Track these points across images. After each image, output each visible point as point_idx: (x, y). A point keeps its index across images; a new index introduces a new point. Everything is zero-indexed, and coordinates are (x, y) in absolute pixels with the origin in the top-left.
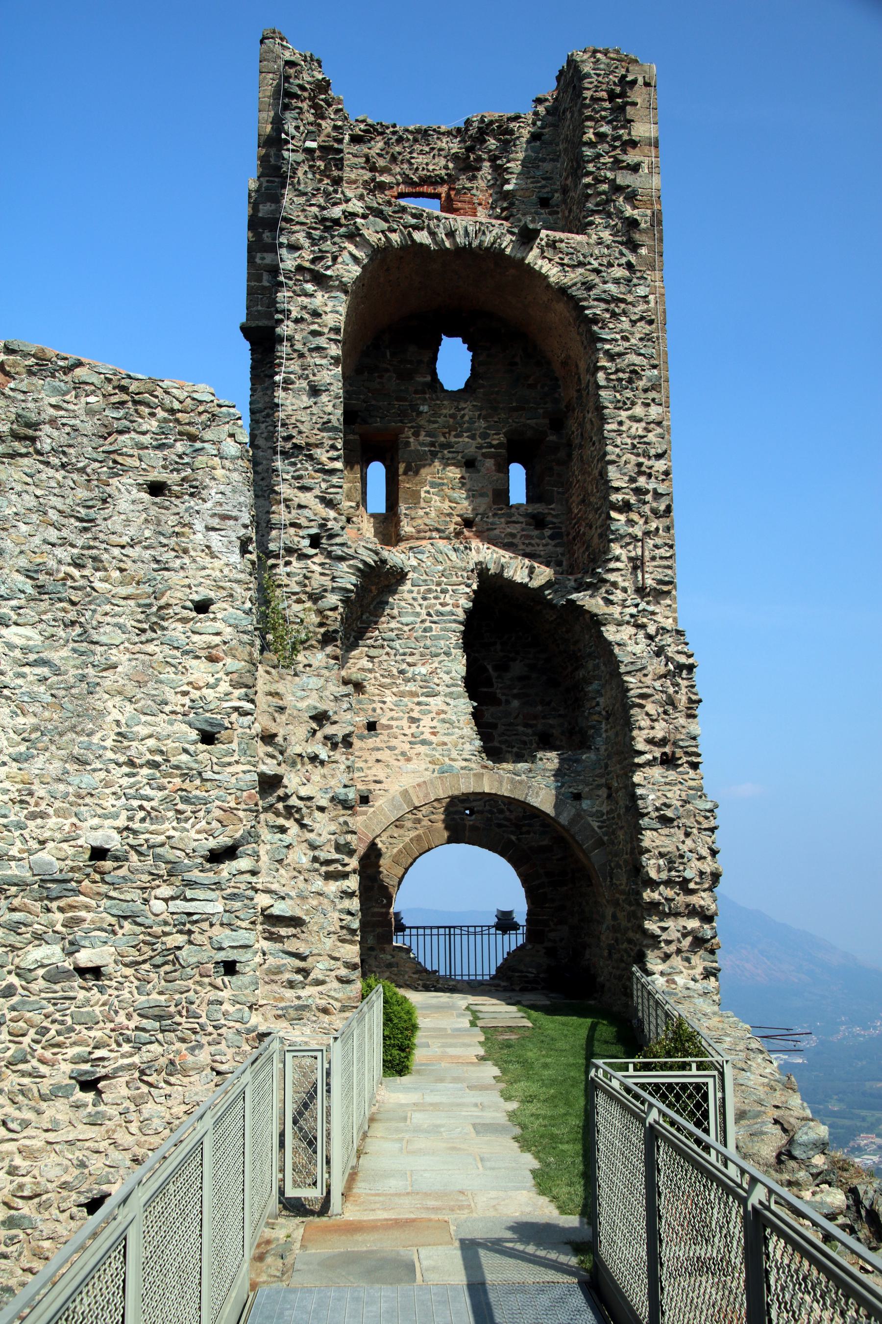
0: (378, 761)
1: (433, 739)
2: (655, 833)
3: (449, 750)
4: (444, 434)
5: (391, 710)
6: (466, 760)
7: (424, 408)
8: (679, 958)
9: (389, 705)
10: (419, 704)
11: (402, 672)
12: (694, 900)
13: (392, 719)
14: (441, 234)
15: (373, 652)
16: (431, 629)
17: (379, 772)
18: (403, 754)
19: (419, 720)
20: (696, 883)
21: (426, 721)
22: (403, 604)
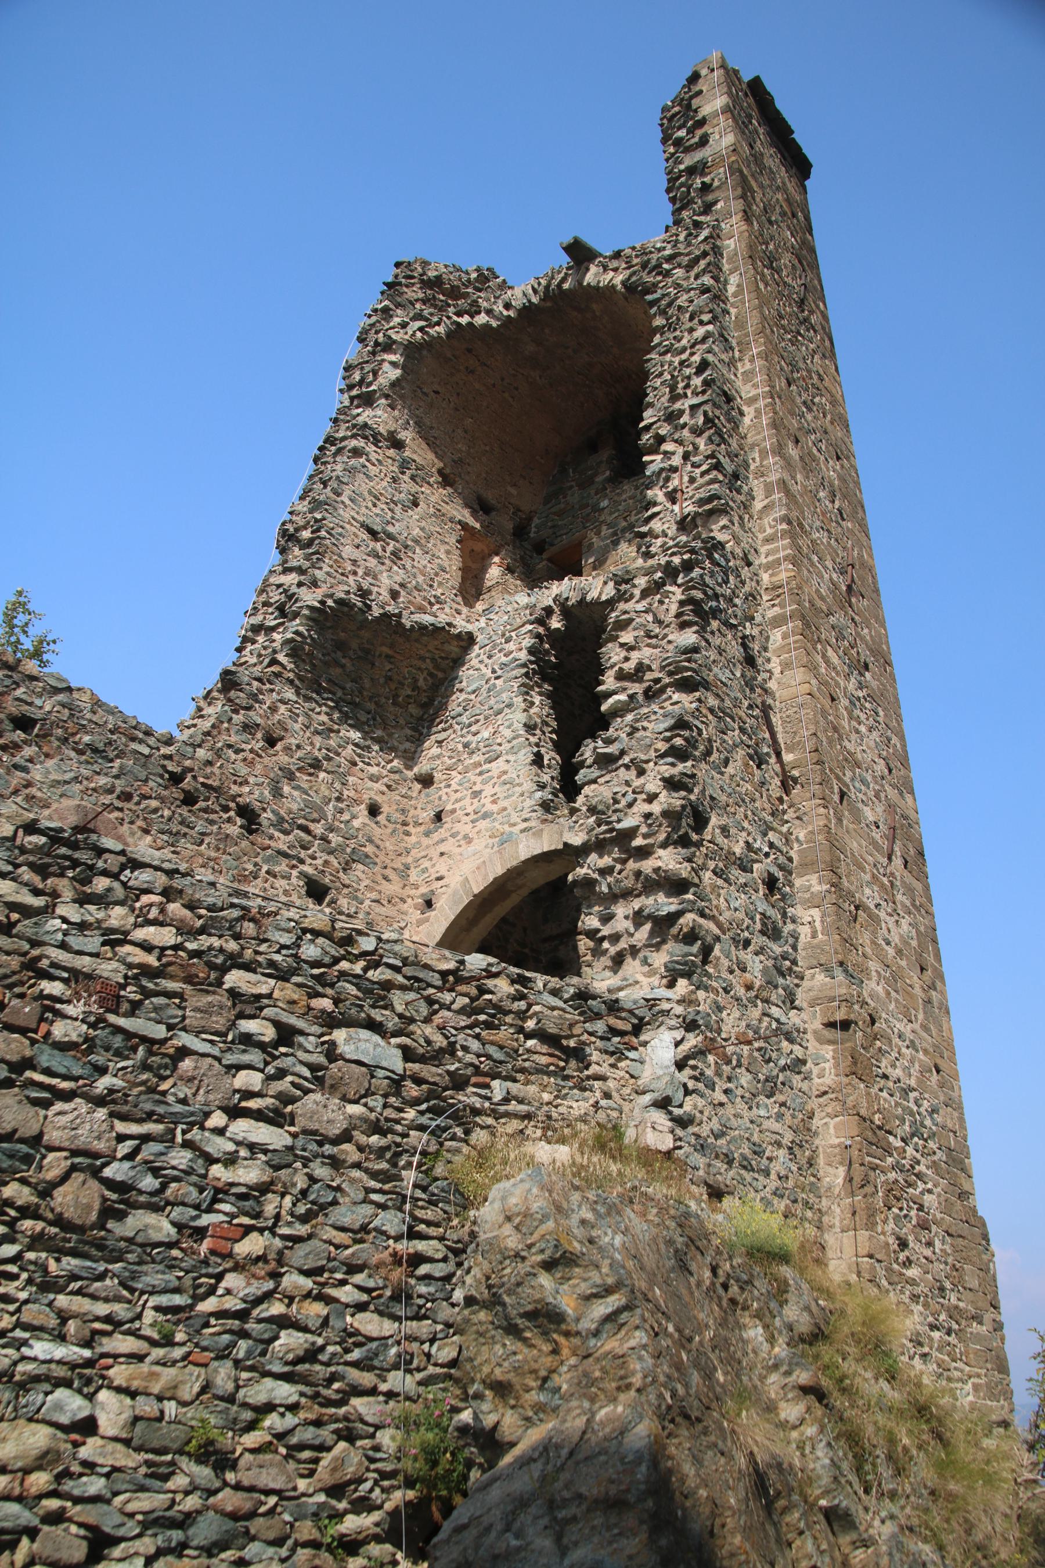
0: (442, 854)
1: (495, 808)
2: (593, 786)
3: (509, 815)
4: (625, 519)
5: (456, 791)
6: (525, 820)
7: (605, 503)
8: (637, 962)
9: (454, 786)
10: (481, 774)
11: (466, 746)
12: (647, 866)
13: (457, 801)
14: (499, 308)
15: (441, 736)
16: (494, 685)
17: (441, 867)
18: (466, 837)
19: (480, 792)
20: (645, 836)
21: (488, 790)
22: (471, 672)
